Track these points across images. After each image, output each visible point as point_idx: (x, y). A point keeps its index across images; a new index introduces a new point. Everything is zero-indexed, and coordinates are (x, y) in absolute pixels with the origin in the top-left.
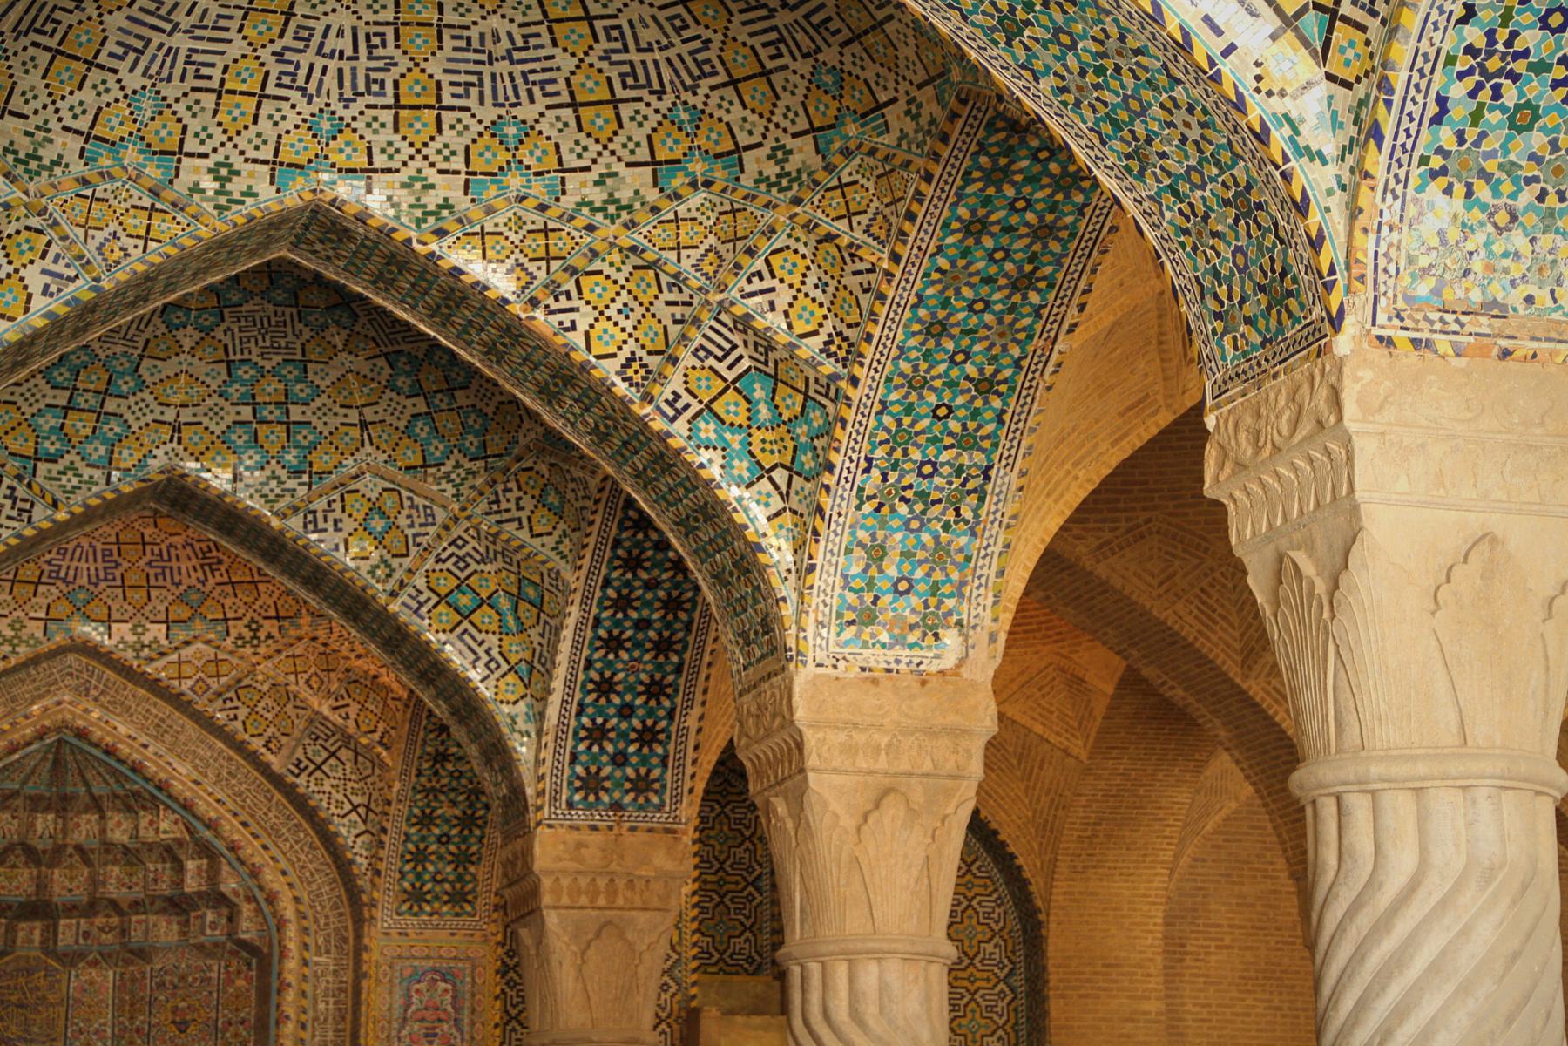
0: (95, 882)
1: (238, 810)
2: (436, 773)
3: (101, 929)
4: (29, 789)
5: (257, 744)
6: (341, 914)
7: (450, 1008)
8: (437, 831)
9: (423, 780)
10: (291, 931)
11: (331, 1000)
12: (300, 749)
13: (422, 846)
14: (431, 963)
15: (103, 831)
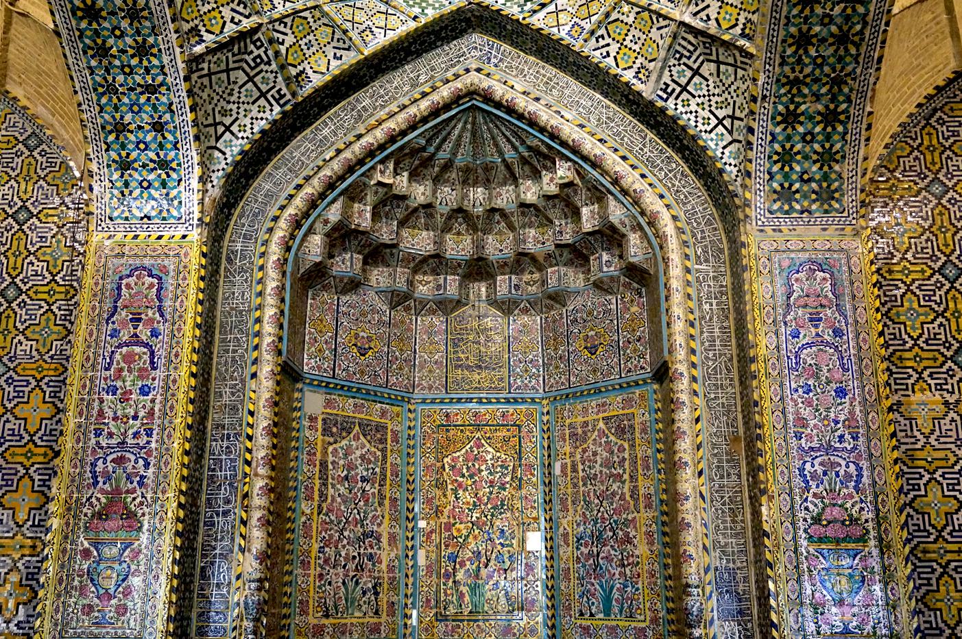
0: (519, 241)
1: (618, 147)
2: (800, 61)
3: (527, 283)
4: (460, 161)
5: (628, 76)
6: (715, 229)
7: (830, 295)
8: (801, 129)
9: (787, 69)
10: (673, 244)
11: (714, 302)
12: (667, 73)
13: (788, 146)
14: (807, 255)
15: (518, 196)
